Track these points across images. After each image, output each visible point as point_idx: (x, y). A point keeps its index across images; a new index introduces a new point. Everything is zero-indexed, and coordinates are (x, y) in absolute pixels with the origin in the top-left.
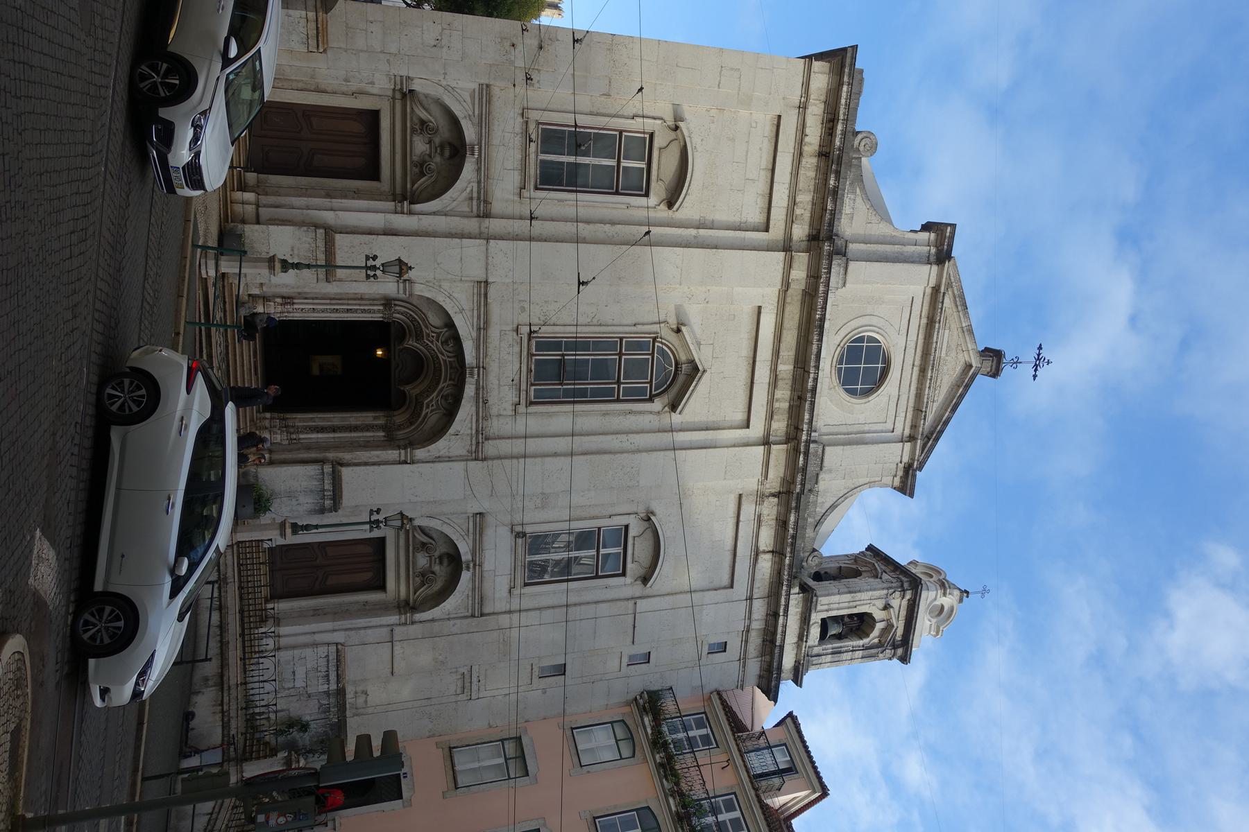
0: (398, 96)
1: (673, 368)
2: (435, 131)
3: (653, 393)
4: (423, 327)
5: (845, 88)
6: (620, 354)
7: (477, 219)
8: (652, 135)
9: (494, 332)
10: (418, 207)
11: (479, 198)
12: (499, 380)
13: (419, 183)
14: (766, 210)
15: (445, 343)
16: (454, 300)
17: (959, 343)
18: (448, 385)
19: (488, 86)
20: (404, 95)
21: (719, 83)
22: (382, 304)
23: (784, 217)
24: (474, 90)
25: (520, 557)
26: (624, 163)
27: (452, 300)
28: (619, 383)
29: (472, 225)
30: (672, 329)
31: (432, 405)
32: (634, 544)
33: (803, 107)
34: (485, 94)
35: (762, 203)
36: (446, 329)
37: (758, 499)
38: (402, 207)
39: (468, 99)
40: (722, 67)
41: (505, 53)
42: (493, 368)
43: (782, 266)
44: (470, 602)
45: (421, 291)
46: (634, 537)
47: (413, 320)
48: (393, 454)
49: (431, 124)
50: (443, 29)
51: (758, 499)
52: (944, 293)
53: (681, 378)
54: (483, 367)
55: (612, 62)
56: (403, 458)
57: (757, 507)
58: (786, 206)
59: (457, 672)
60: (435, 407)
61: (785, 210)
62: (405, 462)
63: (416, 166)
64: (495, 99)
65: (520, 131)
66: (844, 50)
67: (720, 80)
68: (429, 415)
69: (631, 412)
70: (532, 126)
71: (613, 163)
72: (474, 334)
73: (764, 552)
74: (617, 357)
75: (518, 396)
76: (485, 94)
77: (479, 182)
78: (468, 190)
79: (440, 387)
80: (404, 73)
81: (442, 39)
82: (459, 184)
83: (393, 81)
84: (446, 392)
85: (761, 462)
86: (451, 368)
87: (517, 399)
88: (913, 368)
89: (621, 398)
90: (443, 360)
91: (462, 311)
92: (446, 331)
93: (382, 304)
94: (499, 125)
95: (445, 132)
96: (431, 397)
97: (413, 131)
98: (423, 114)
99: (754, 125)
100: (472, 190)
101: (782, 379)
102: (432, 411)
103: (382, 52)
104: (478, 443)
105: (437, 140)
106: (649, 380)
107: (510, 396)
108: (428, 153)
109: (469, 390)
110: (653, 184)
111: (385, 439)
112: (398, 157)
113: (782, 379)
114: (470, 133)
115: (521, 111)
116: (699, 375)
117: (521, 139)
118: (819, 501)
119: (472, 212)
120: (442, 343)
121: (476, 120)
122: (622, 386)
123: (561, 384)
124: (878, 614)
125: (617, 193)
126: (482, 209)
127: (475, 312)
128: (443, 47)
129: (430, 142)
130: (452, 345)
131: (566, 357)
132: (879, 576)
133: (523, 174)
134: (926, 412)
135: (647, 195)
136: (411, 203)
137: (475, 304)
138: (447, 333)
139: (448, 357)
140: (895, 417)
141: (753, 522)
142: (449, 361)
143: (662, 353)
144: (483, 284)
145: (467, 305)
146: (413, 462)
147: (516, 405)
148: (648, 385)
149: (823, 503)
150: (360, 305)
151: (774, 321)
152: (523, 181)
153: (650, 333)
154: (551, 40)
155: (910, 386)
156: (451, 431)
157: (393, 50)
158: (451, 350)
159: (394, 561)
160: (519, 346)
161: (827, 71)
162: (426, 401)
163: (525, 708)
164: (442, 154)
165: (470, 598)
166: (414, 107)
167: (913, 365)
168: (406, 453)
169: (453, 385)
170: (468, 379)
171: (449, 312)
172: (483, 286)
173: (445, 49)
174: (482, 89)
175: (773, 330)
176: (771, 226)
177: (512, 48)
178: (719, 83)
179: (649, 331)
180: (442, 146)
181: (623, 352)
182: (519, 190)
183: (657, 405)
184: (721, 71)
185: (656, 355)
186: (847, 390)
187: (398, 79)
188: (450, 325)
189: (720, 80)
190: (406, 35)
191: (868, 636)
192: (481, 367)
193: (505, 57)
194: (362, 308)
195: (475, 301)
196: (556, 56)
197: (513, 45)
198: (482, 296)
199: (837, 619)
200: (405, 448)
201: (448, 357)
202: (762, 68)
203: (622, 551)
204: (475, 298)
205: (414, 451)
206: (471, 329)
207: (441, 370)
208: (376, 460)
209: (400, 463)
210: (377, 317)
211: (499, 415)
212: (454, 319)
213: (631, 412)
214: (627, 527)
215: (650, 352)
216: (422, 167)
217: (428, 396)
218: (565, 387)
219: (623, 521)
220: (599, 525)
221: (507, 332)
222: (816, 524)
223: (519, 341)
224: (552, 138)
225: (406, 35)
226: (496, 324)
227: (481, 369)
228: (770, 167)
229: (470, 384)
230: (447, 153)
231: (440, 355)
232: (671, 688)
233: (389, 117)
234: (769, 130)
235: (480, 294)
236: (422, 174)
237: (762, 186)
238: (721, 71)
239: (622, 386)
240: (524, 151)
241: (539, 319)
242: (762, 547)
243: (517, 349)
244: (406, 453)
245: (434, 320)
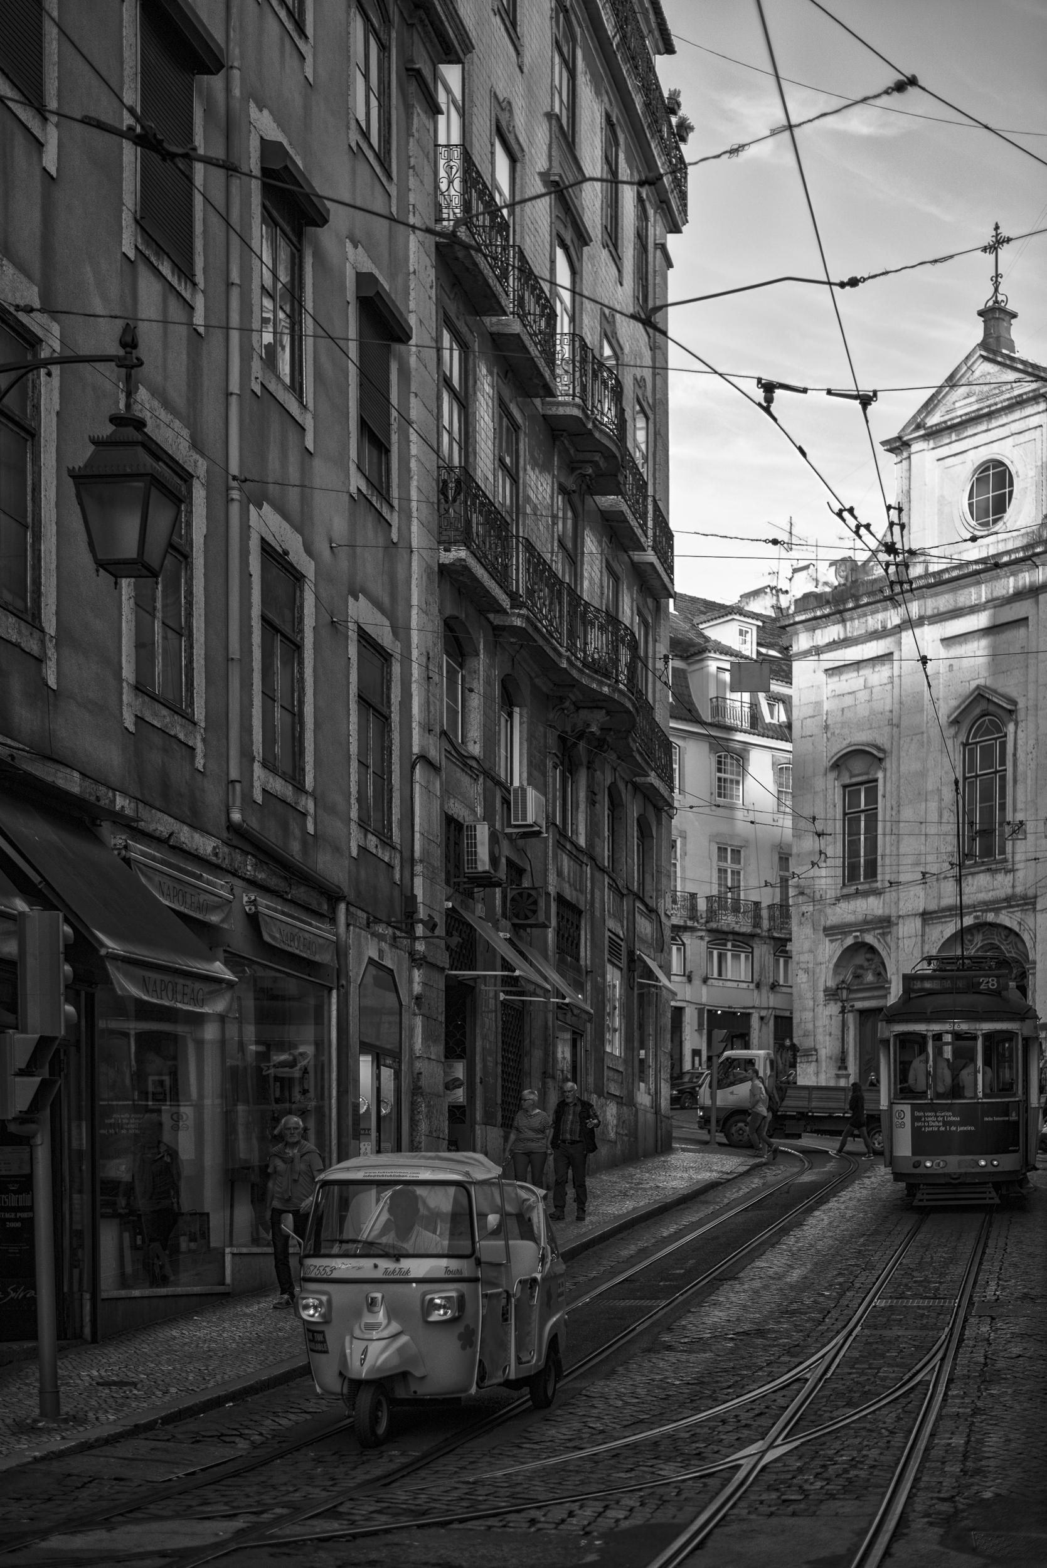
6: (977, 776)
8: (845, 787)
28: (996, 772)
34: (832, 931)
53: (992, 708)
69: (1015, 755)
70: (845, 891)
76: (832, 931)
77: (874, 929)
82: (876, 945)
97: (862, 984)
104: (1026, 904)
105: (866, 964)
107: (1000, 877)
109: (990, 917)
114: (850, 941)
135: (876, 780)
143: (974, 737)
145: (939, 928)
156: (1016, 928)
172: (927, 917)
183: (1011, 727)
211: (1013, 887)
213: (1015, 755)
224: (851, 873)
237: (866, 672)
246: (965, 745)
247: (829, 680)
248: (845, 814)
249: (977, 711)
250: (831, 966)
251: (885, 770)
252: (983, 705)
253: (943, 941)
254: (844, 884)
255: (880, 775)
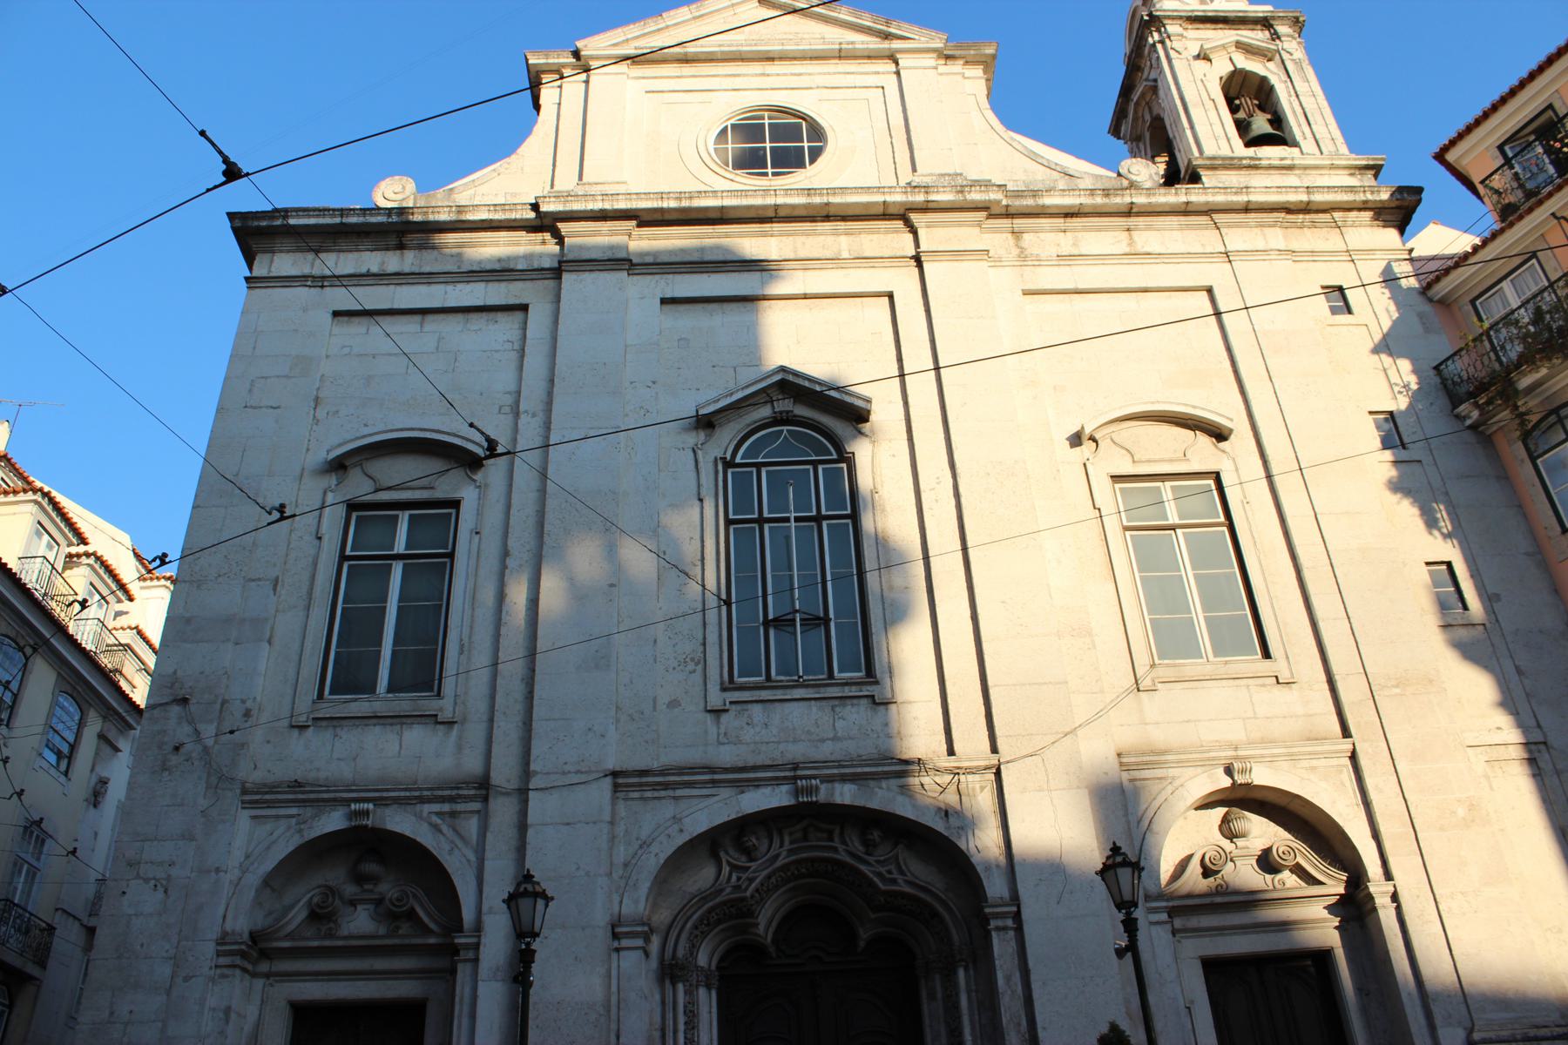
0: (264, 967)
1: (785, 428)
2: (330, 891)
3: (835, 457)
4: (718, 900)
5: (292, 221)
6: (761, 521)
7: (491, 800)
8: (352, 506)
9: (727, 756)
10: (468, 915)
11: (451, 799)
12: (823, 741)
13: (425, 919)
14: (492, 315)
15: (749, 853)
16: (656, 834)
17: (722, 21)
18: (844, 842)
19: (245, 792)
20: (266, 955)
21: (272, 407)
22: (674, 984)
23: (503, 285)
24: (254, 817)
25: (1208, 670)
26: (400, 547)
27: (653, 839)
29: (503, 811)
30: (709, 437)
31: (890, 872)
32: (1149, 461)
33: (320, 281)
34: (261, 798)
35: (478, 321)
36: (722, 854)
37: (1030, 263)
38: (467, 947)
39: (268, 827)
40: (246, 407)
41: (190, 763)
42: (796, 752)
43: (587, 274)
44: (1323, 762)
45: (636, 902)
46: (1134, 462)
47: (705, 926)
48: (1002, 947)
49: (315, 900)
50: (138, 877)
51: (1030, 263)
52: (636, 48)
53: (802, 411)
54: (795, 769)
55: (220, 579)
56: (1010, 923)
57: (1042, 263)
58: (482, 285)
59: (1487, 777)
60: (892, 867)
61: (491, 284)
62: (1017, 916)
63: (398, 928)
64: (271, 779)
65: (330, 731)
66: (236, 231)
67: (267, 407)
68: (909, 877)
70: (325, 711)
71: (397, 570)
72: (725, 793)
73: (1131, 242)
74: (766, 527)
75: (855, 701)
76: (261, 798)
77: (422, 800)
78: (435, 819)
79: (848, 859)
80: (210, 948)
81: (154, 879)
83: (226, 971)
84: (859, 848)
85: (956, 264)
86: (805, 839)
87: (864, 702)
88: (768, 75)
89: (849, 512)
90: (787, 857)
91: (676, 819)
92: (727, 853)
93: (674, 984)
94: (318, 770)
95: (335, 875)
96: (871, 876)
97: (330, 936)
98: (298, 915)
99: (346, 350)
100: (438, 814)
101: (795, 252)
102: (902, 873)
103: (168, 992)
105: (350, 890)
106: (810, 467)
108: (371, 907)
109: (845, 794)
110: (439, 494)
111: (971, 965)
112: (380, 964)
113: (795, 252)
114: (334, 821)
115: (296, 732)
116: (791, 378)
117: (346, 729)
118: (1024, 178)
119: (478, 812)
120: (752, 860)
121: (309, 812)
122: (824, 512)
123: (826, 621)
124: (1222, 67)
125: (451, 556)
126: (472, 792)
127: (679, 793)
128: (169, 876)
129: (353, 903)
130: (754, 841)
131: (771, 617)
132: (1152, 84)
133: (409, 720)
134: (840, 44)
135: (455, 504)
136: (460, 929)
137: (663, 793)
138: (731, 852)
139: (781, 846)
140: (855, 87)
141: (1073, 267)
142: (791, 843)
143: (753, 451)
144: (620, 781)
145: (667, 809)
146: (1015, 898)
147: (874, 703)
148: (820, 468)
149: (1025, 171)
150: (675, 1031)
151: (687, 276)
152: (423, 720)
153: (716, 472)
154: (173, 684)
155: (800, 74)
157: (168, 971)
158: (766, 842)
159: (1254, 936)
160: (750, 706)
161: (268, 256)
162: (881, 885)
163: (1541, 632)
164: (374, 879)
165: (1315, 763)
166: (282, 934)
167: (763, 75)
168: (997, 916)
169: (842, 834)
170: (822, 796)
171: (681, 843)
172: (622, 781)
173: (175, 872)
174: (251, 802)
175: (705, 276)
176: (517, 302)
177: (182, 750)
178: (272, 407)
179: (712, 476)
180: (360, 879)
181: (756, 516)
182: (438, 726)
184: (251, 407)
185: (760, 460)
186: (812, 161)
187: (223, 961)
188: (711, 842)
189: (267, 407)
190: (142, 945)
191: (1264, 80)
192: (791, 772)
193: (196, 763)
194: (681, 1027)
195: (656, 794)
196: (202, 673)
197: (177, 749)
198: (644, 780)
199: (1242, 127)
200: (985, 920)
201: (781, 846)
202: (254, 348)
203: (1168, 484)
204: (649, 794)
205: (989, 900)
206: (716, 798)
207: (813, 860)
208: (1017, 978)
209: (1019, 929)
210: (707, 1004)
212: (695, 835)
214: (1116, 478)
215: (754, 470)
216: (395, 915)
217: (871, 884)
218: (832, 615)
219: (1103, 488)
220: (1119, 529)
221: (722, 730)
222: (1067, 177)
223: (739, 707)
225: (142, 945)
226: (706, 753)
227: (799, 773)
228: (418, 318)
229: (832, 794)
230: (371, 867)
231: (778, 864)
232: (1436, 368)
233: (308, 985)
234: (357, 327)
235: (641, 785)
236: (411, 915)
237: (451, 325)
238: (251, 407)
239: (824, 512)
240: (366, 721)
241: (694, 671)
242: (1123, 248)
243: (757, 709)
244: (997, 916)
245: (703, 876)
246: (729, 464)
247: (336, 330)
248: (343, 558)
249: (765, 412)
250: (254, 879)
251: (482, 488)
252: (785, 405)
253: (685, 837)
254: (321, 695)
255: (468, 495)
